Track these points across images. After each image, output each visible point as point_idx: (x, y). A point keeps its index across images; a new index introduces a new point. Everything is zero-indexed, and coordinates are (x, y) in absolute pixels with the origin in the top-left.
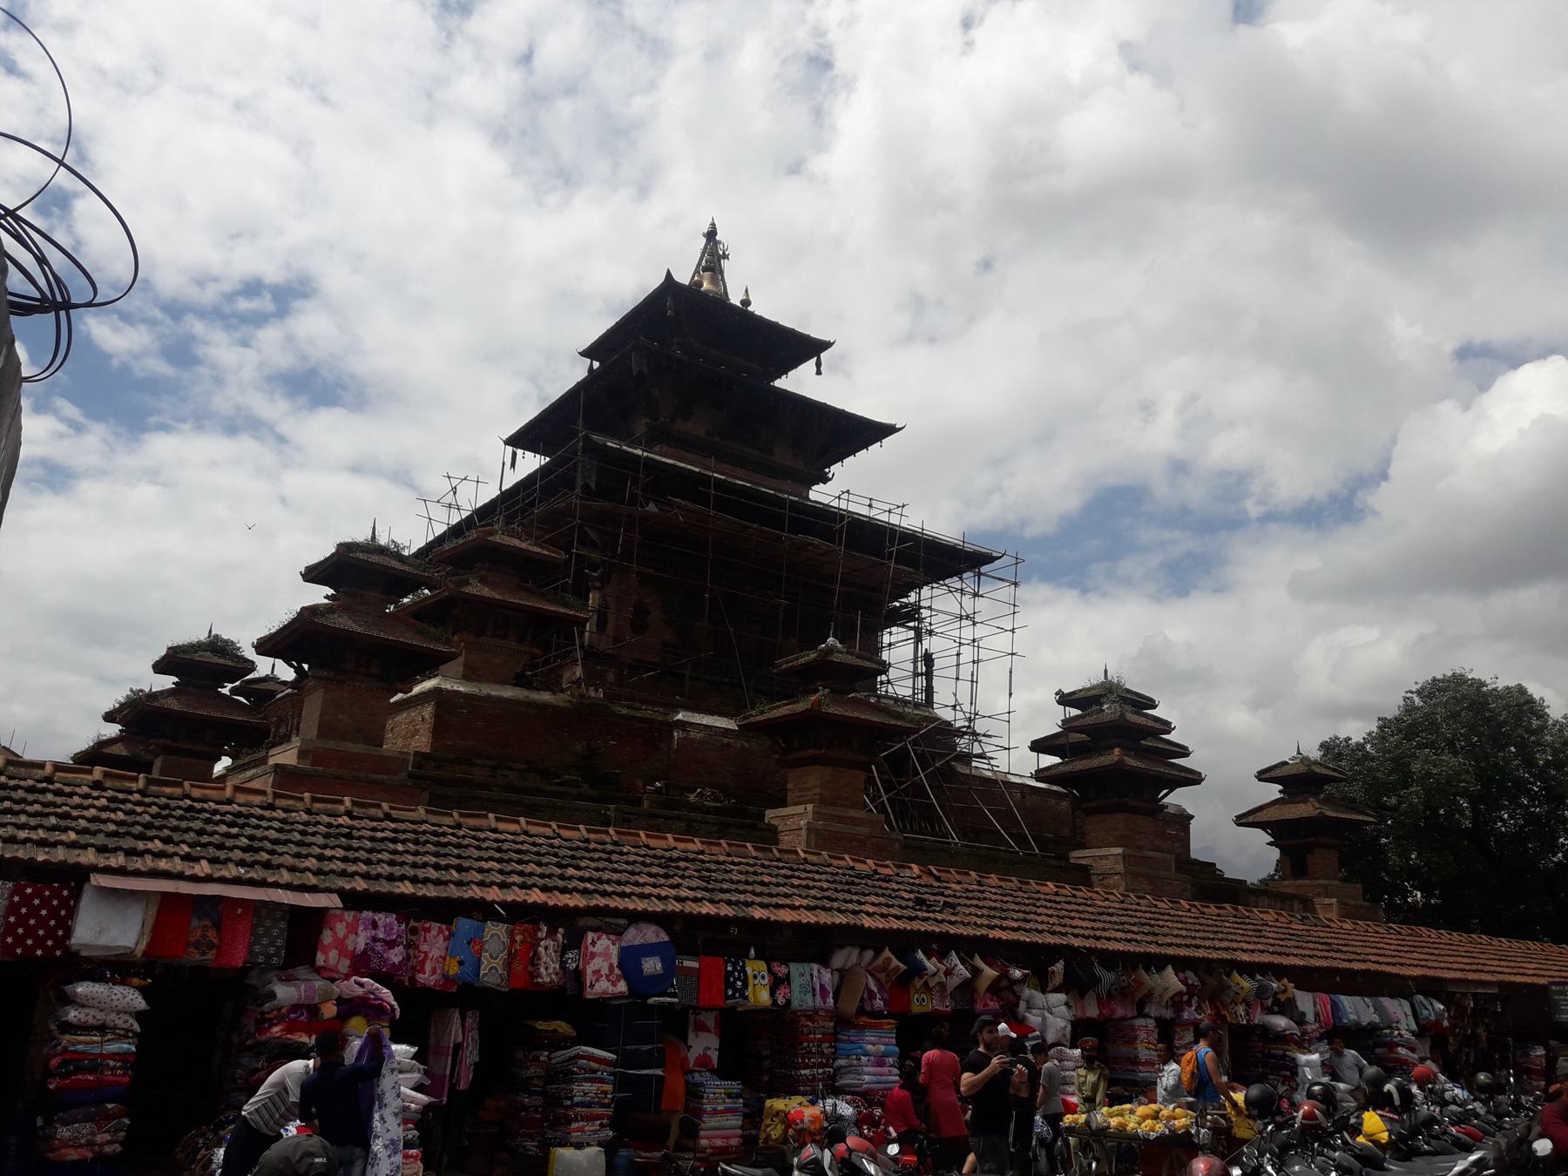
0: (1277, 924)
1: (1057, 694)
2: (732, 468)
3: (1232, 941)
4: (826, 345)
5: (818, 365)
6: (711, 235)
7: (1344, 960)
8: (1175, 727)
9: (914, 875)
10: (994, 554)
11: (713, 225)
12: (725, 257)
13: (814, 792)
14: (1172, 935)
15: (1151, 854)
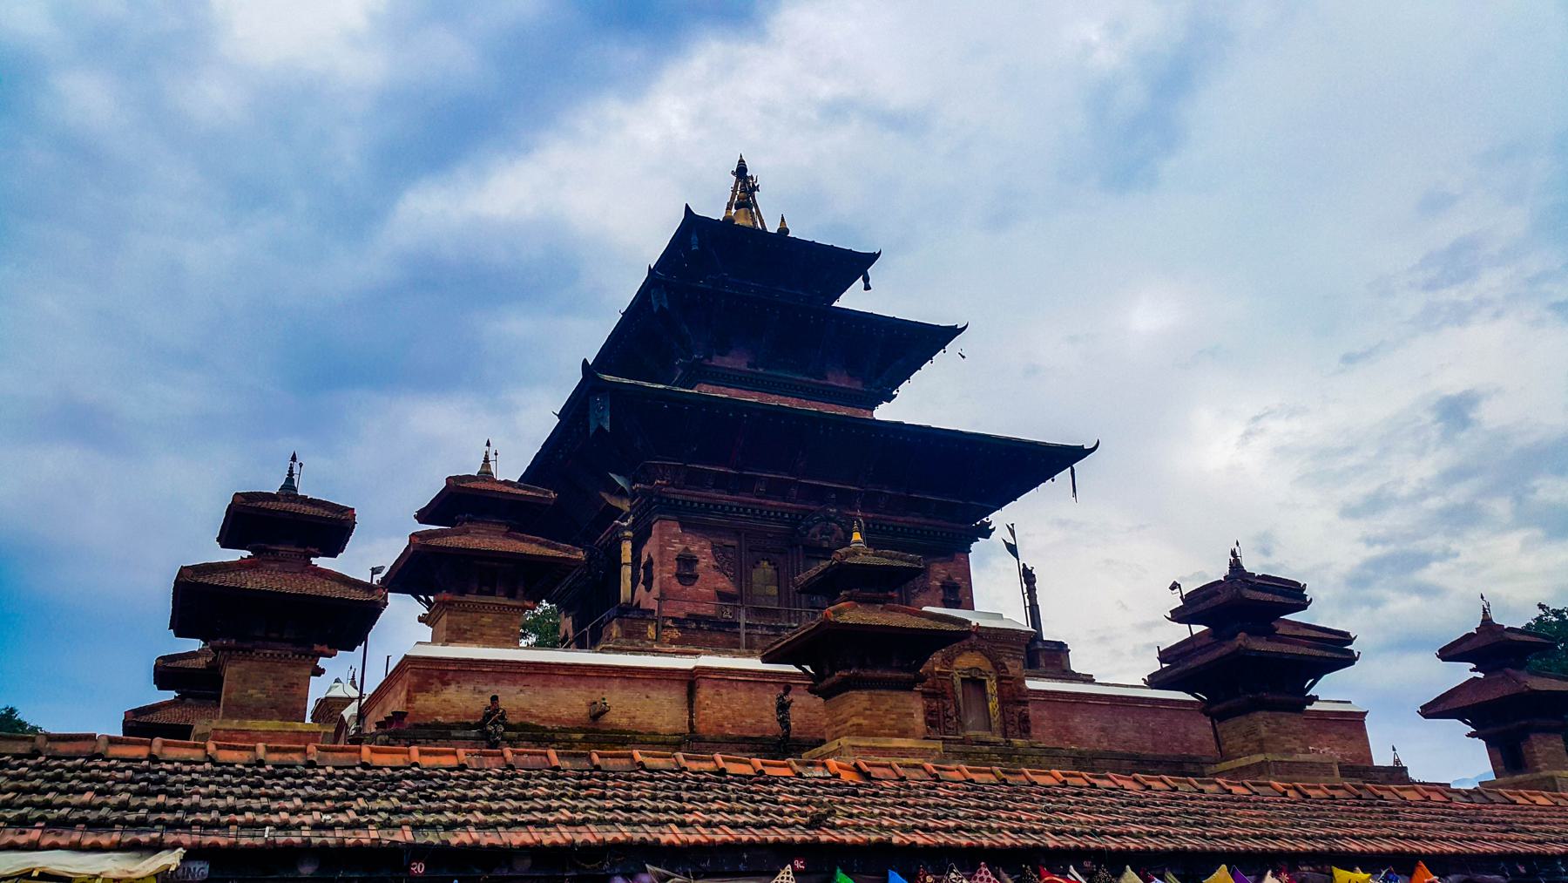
0: (1429, 803)
1: (1173, 588)
2: (781, 398)
3: (1338, 826)
4: (872, 258)
5: (866, 280)
6: (741, 171)
7: (1530, 842)
8: (1311, 599)
9: (829, 775)
10: (1085, 448)
11: (741, 161)
12: (756, 188)
13: (849, 724)
14: (1237, 824)
15: (1302, 757)
